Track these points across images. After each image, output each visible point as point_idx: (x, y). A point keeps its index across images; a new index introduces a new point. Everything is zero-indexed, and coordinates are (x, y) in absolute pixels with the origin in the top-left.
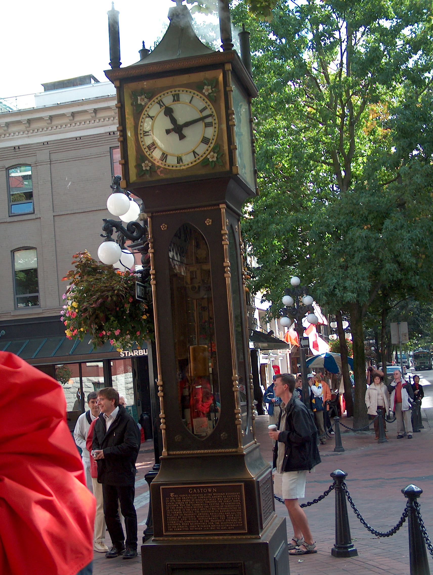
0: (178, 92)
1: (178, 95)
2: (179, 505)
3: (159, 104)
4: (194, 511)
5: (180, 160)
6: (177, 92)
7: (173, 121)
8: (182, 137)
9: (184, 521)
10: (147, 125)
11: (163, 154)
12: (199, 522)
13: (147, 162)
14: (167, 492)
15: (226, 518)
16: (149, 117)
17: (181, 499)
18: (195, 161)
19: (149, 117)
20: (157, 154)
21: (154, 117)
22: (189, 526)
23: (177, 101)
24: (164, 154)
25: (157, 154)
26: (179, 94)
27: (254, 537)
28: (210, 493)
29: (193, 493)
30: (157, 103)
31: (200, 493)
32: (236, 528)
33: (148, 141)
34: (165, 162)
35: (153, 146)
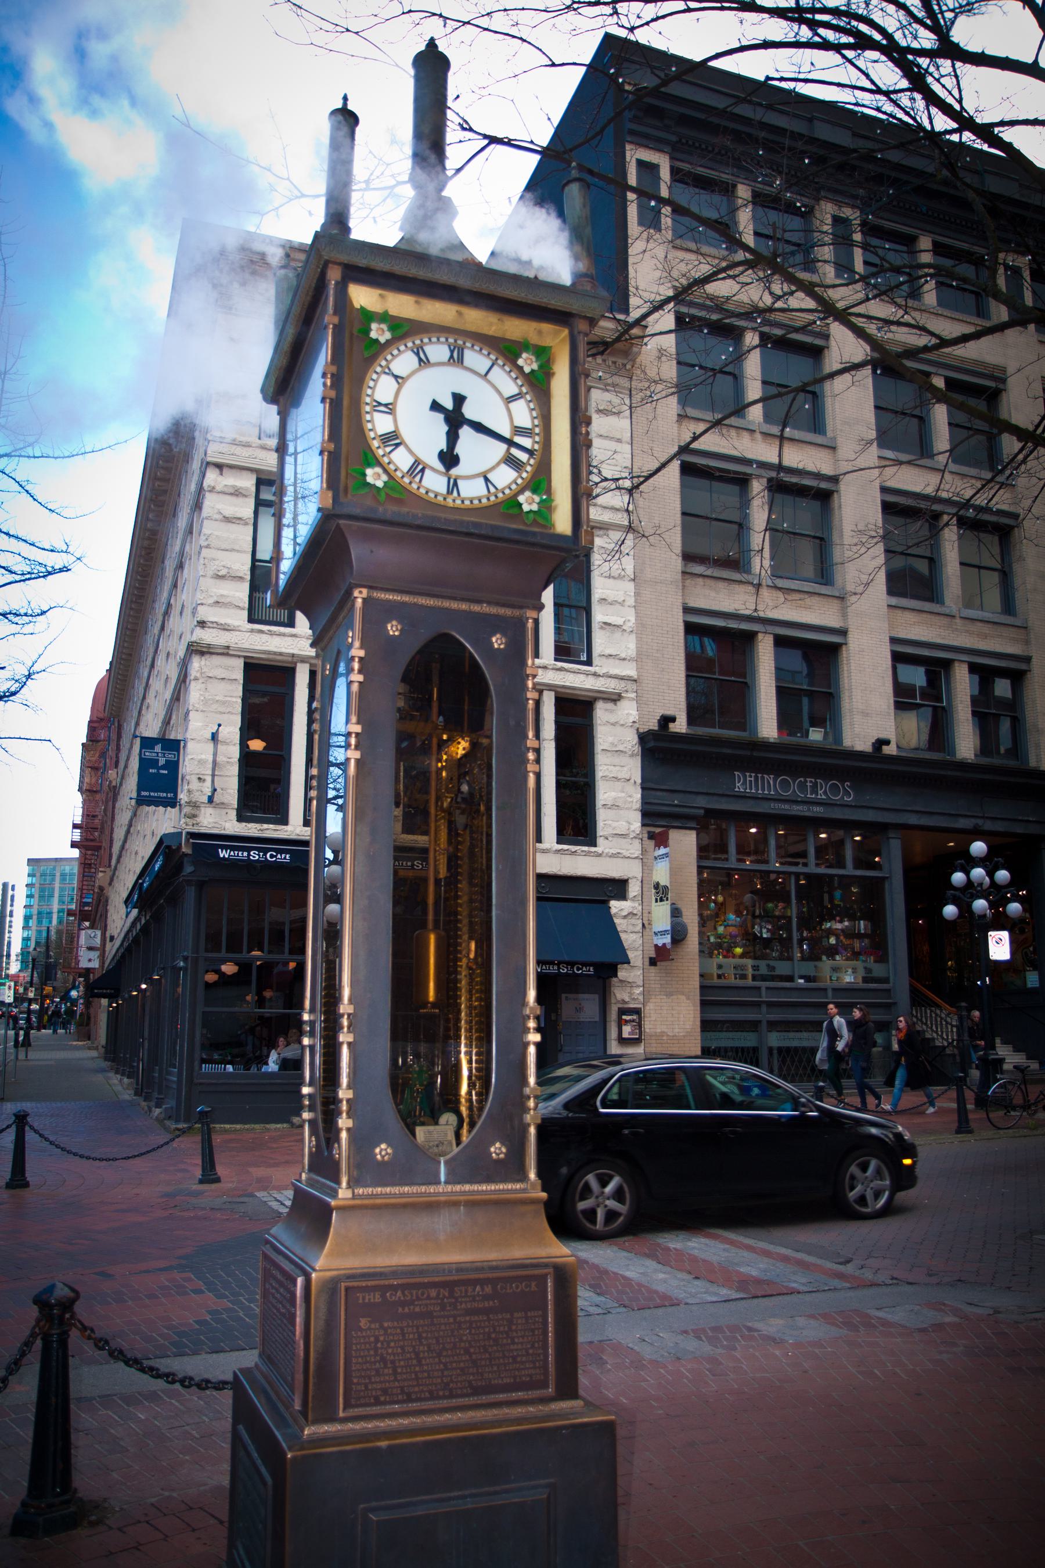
10: (383, 389)
11: (417, 462)
21: (402, 378)
33: (382, 424)
35: (393, 439)
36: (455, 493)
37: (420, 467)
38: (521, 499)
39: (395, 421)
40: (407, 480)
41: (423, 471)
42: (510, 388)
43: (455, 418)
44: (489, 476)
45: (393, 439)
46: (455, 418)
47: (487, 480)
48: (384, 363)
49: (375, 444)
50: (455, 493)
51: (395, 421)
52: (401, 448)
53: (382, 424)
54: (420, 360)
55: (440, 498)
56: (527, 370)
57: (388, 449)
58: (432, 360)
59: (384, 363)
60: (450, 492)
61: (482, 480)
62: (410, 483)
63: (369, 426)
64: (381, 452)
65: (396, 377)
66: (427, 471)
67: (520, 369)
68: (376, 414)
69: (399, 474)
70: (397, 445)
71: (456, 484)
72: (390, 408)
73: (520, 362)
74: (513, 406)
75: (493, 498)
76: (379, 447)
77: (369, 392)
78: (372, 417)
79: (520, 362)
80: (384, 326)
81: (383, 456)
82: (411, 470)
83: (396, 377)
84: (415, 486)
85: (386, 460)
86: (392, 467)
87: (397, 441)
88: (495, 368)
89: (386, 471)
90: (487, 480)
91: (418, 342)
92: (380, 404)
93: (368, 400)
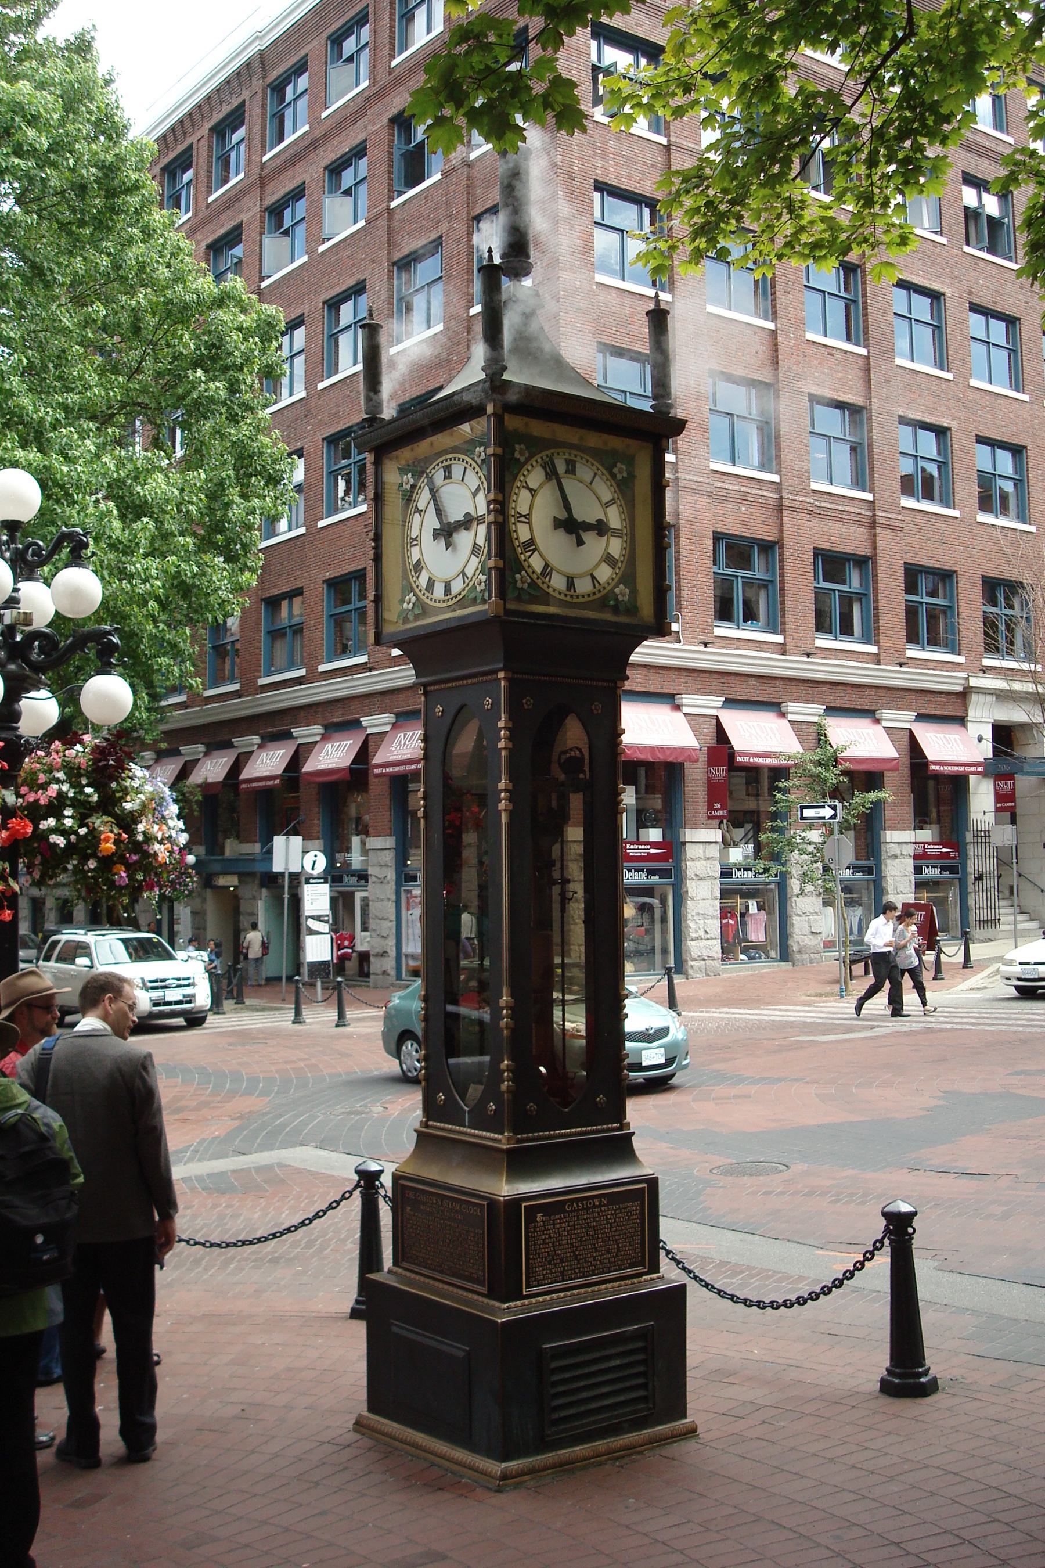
2: (550, 1237)
4: (572, 1244)
5: (570, 584)
9: (555, 1265)
10: (522, 502)
11: (547, 565)
12: (579, 1263)
13: (523, 573)
14: (531, 1211)
15: (618, 1250)
16: (527, 487)
17: (554, 1224)
18: (594, 594)
19: (527, 487)
21: (535, 491)
22: (562, 1273)
25: (536, 563)
27: (655, 1276)
28: (597, 1207)
29: (571, 1211)
31: (583, 1209)
32: (632, 1265)
35: (530, 545)
38: (617, 590)
39: (531, 529)
41: (551, 573)
42: (606, 495)
48: (522, 478)
49: (519, 550)
51: (531, 529)
53: (523, 533)
56: (619, 477)
59: (522, 478)
60: (569, 589)
65: (531, 490)
68: (518, 524)
69: (535, 576)
70: (534, 551)
71: (573, 583)
72: (528, 518)
73: (615, 470)
77: (513, 505)
79: (615, 470)
83: (531, 490)
85: (526, 564)
86: (530, 571)
88: (597, 478)
90: (593, 577)
92: (522, 516)
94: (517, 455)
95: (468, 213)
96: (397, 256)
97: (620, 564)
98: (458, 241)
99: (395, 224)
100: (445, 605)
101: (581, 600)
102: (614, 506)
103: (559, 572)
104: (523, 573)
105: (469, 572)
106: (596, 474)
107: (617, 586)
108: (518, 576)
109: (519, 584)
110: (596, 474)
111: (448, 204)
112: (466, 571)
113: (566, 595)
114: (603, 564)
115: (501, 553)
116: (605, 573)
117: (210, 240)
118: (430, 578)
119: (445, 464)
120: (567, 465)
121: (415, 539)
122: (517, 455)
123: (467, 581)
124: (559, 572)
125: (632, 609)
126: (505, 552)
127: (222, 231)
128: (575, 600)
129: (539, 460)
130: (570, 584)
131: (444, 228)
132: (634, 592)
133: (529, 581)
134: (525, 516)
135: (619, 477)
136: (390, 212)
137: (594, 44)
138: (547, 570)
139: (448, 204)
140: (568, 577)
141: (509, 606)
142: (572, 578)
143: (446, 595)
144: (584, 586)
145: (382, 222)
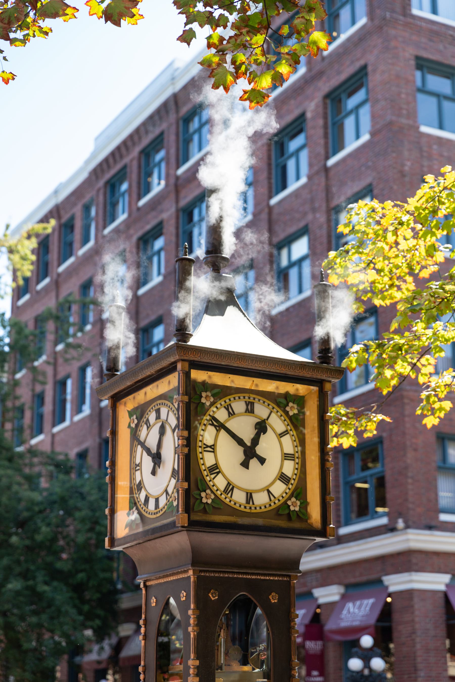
0: (253, 401)
1: (252, 404)
3: (227, 409)
5: (249, 497)
6: (251, 400)
7: (255, 441)
8: (245, 464)
11: (229, 484)
13: (208, 491)
20: (220, 483)
23: (251, 413)
24: (230, 484)
25: (220, 483)
26: (253, 403)
30: (225, 407)
33: (209, 459)
34: (231, 497)
35: (215, 469)
36: (251, 503)
37: (231, 487)
38: (289, 503)
40: (223, 496)
41: (232, 489)
43: (250, 453)
44: (271, 489)
45: (215, 469)
46: (250, 453)
47: (269, 492)
49: (205, 473)
50: (251, 503)
52: (220, 475)
53: (209, 459)
54: (229, 413)
55: (242, 507)
56: (291, 413)
57: (213, 476)
58: (236, 412)
60: (248, 502)
61: (266, 492)
62: (226, 498)
63: (201, 462)
64: (208, 479)
66: (235, 489)
67: (287, 413)
68: (205, 453)
70: (218, 473)
72: (213, 448)
73: (288, 409)
74: (283, 439)
75: (272, 504)
76: (207, 476)
78: (203, 456)
79: (288, 409)
80: (209, 394)
81: (210, 481)
82: (226, 491)
84: (228, 500)
87: (217, 470)
89: (212, 492)
90: (269, 492)
91: (227, 401)
92: (207, 446)
93: (200, 444)
94: (203, 400)
95: (328, 206)
96: (276, 240)
97: (292, 481)
98: (320, 227)
99: (274, 216)
100: (154, 516)
101: (258, 510)
102: (288, 436)
103: (240, 489)
104: (208, 491)
105: (170, 490)
106: (271, 412)
107: (289, 499)
108: (203, 494)
109: (204, 500)
110: (271, 412)
111: (312, 200)
112: (168, 489)
113: (245, 507)
114: (278, 482)
115: (187, 478)
116: (279, 489)
117: (140, 233)
118: (146, 496)
119: (157, 407)
120: (247, 405)
121: (138, 465)
122: (203, 400)
123: (168, 497)
124: (240, 489)
125: (303, 515)
126: (191, 474)
127: (148, 227)
128: (253, 511)
129: (223, 403)
130: (249, 497)
131: (310, 217)
132: (305, 504)
133: (213, 497)
134: (210, 447)
135: (291, 413)
136: (270, 209)
137: (418, 74)
138: (230, 488)
139: (312, 200)
140: (247, 493)
141: (195, 517)
142: (251, 494)
143: (156, 509)
144: (261, 499)
145: (264, 216)
